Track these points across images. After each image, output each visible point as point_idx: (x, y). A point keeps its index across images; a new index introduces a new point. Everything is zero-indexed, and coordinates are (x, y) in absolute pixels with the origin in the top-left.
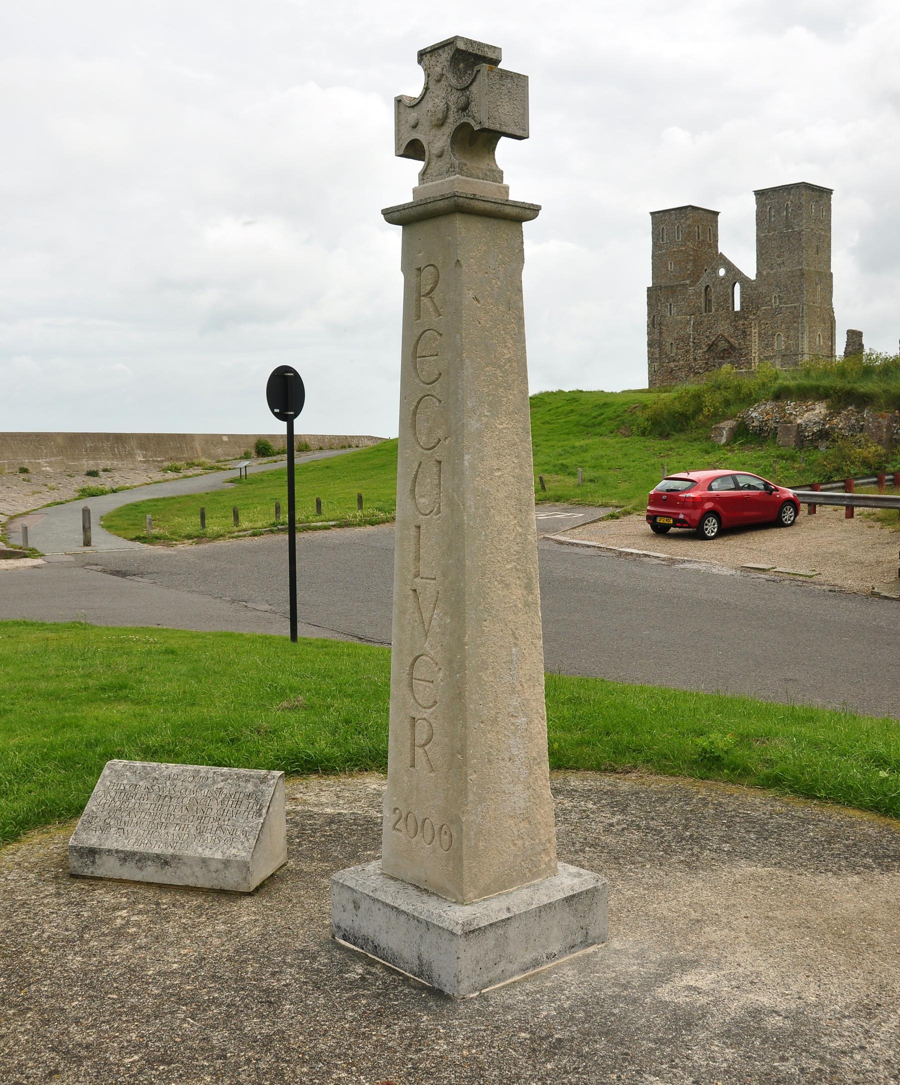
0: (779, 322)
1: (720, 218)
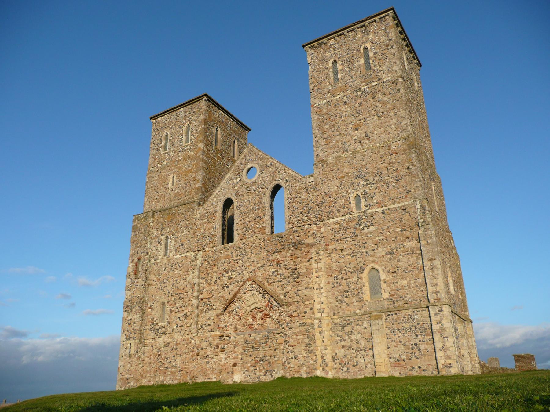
0: (370, 244)
1: (249, 135)
